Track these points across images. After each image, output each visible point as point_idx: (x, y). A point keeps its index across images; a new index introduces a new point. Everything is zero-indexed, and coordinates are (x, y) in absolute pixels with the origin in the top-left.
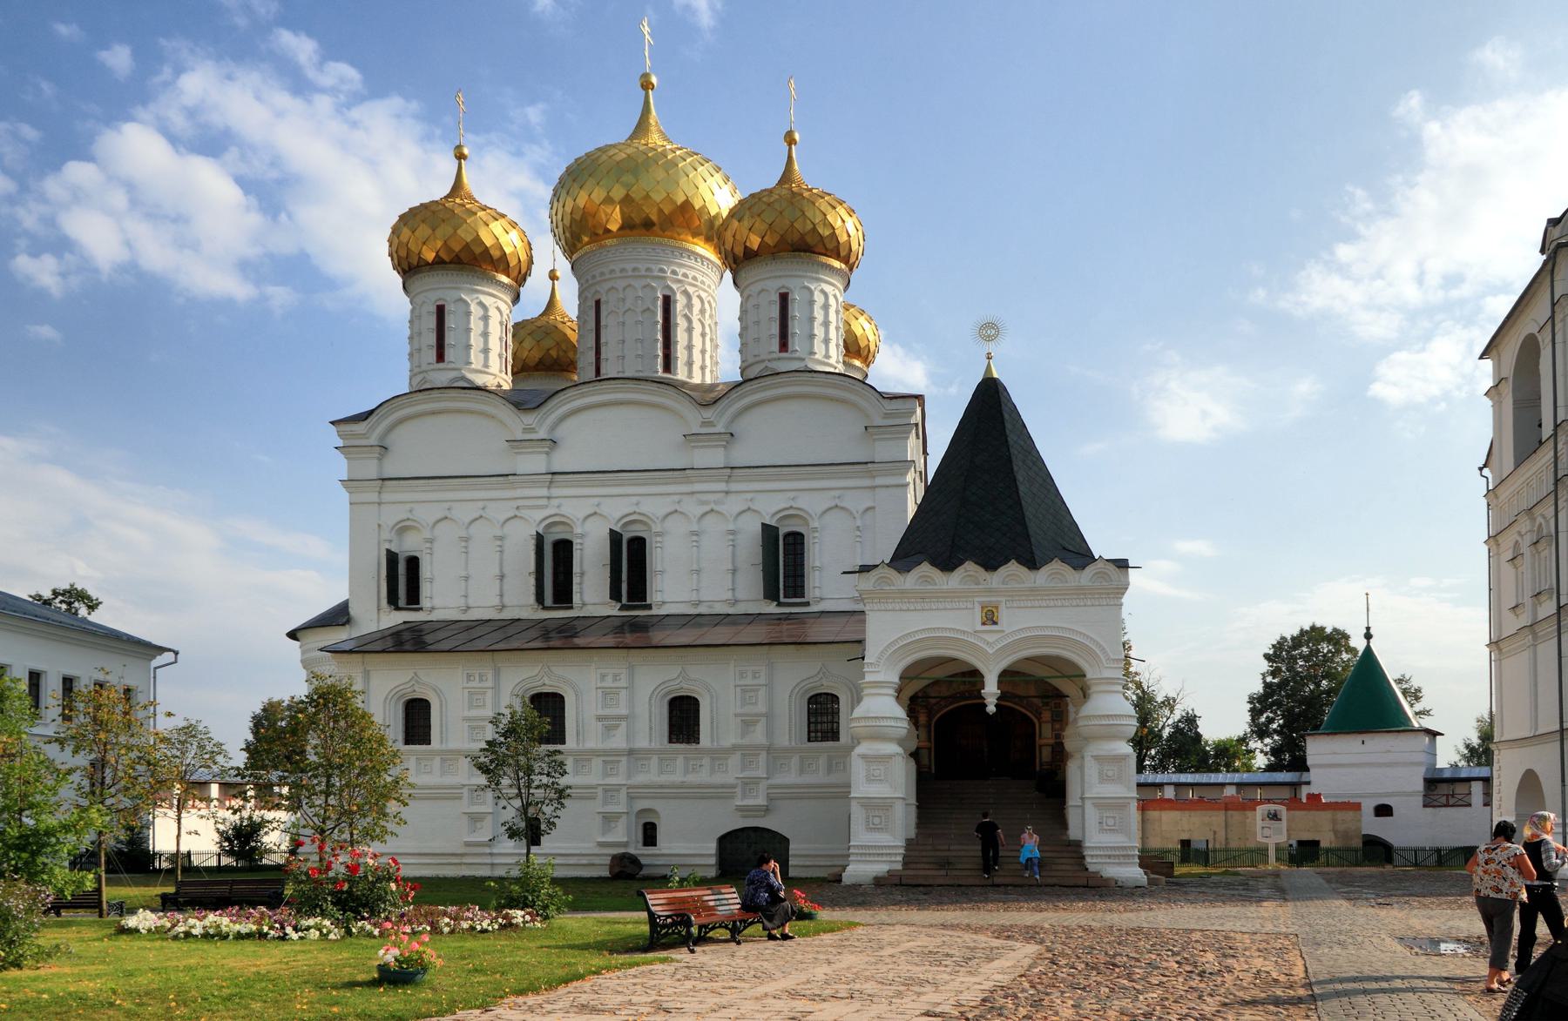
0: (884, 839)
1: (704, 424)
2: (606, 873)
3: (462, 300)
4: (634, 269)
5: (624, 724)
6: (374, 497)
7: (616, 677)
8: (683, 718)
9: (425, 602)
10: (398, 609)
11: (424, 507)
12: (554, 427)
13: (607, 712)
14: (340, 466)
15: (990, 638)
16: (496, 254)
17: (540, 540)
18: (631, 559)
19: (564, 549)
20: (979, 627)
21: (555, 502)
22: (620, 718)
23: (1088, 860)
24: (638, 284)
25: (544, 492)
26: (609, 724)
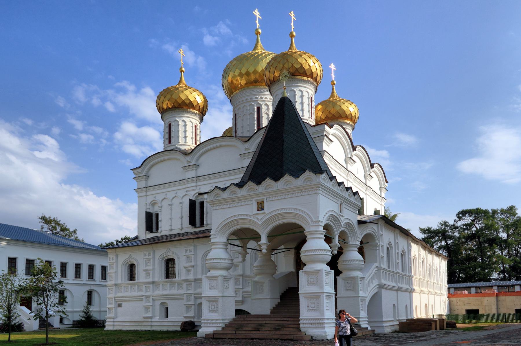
0: (215, 316)
1: (246, 149)
2: (179, 329)
3: (176, 120)
4: (246, 100)
5: (193, 269)
6: (144, 194)
7: (190, 251)
9: (160, 229)
10: (152, 232)
11: (158, 195)
12: (197, 160)
13: (188, 264)
14: (135, 184)
15: (260, 217)
16: (187, 102)
20: (255, 212)
21: (198, 187)
22: (191, 267)
23: (301, 325)
24: (247, 105)
25: (194, 184)
26: (188, 269)
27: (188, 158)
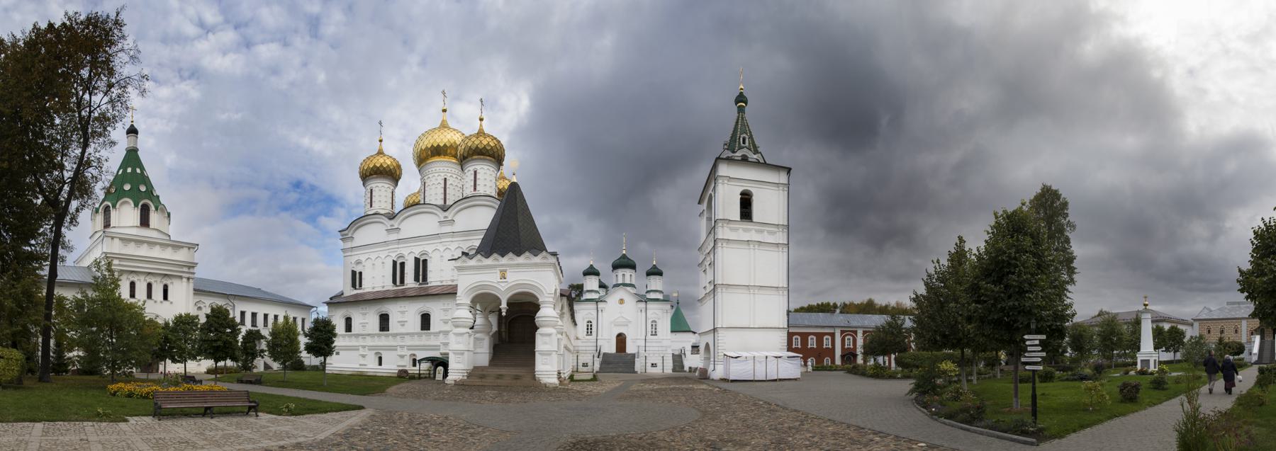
8: (426, 321)
17: (395, 263)
18: (421, 267)
19: (403, 264)
27: (392, 222)
